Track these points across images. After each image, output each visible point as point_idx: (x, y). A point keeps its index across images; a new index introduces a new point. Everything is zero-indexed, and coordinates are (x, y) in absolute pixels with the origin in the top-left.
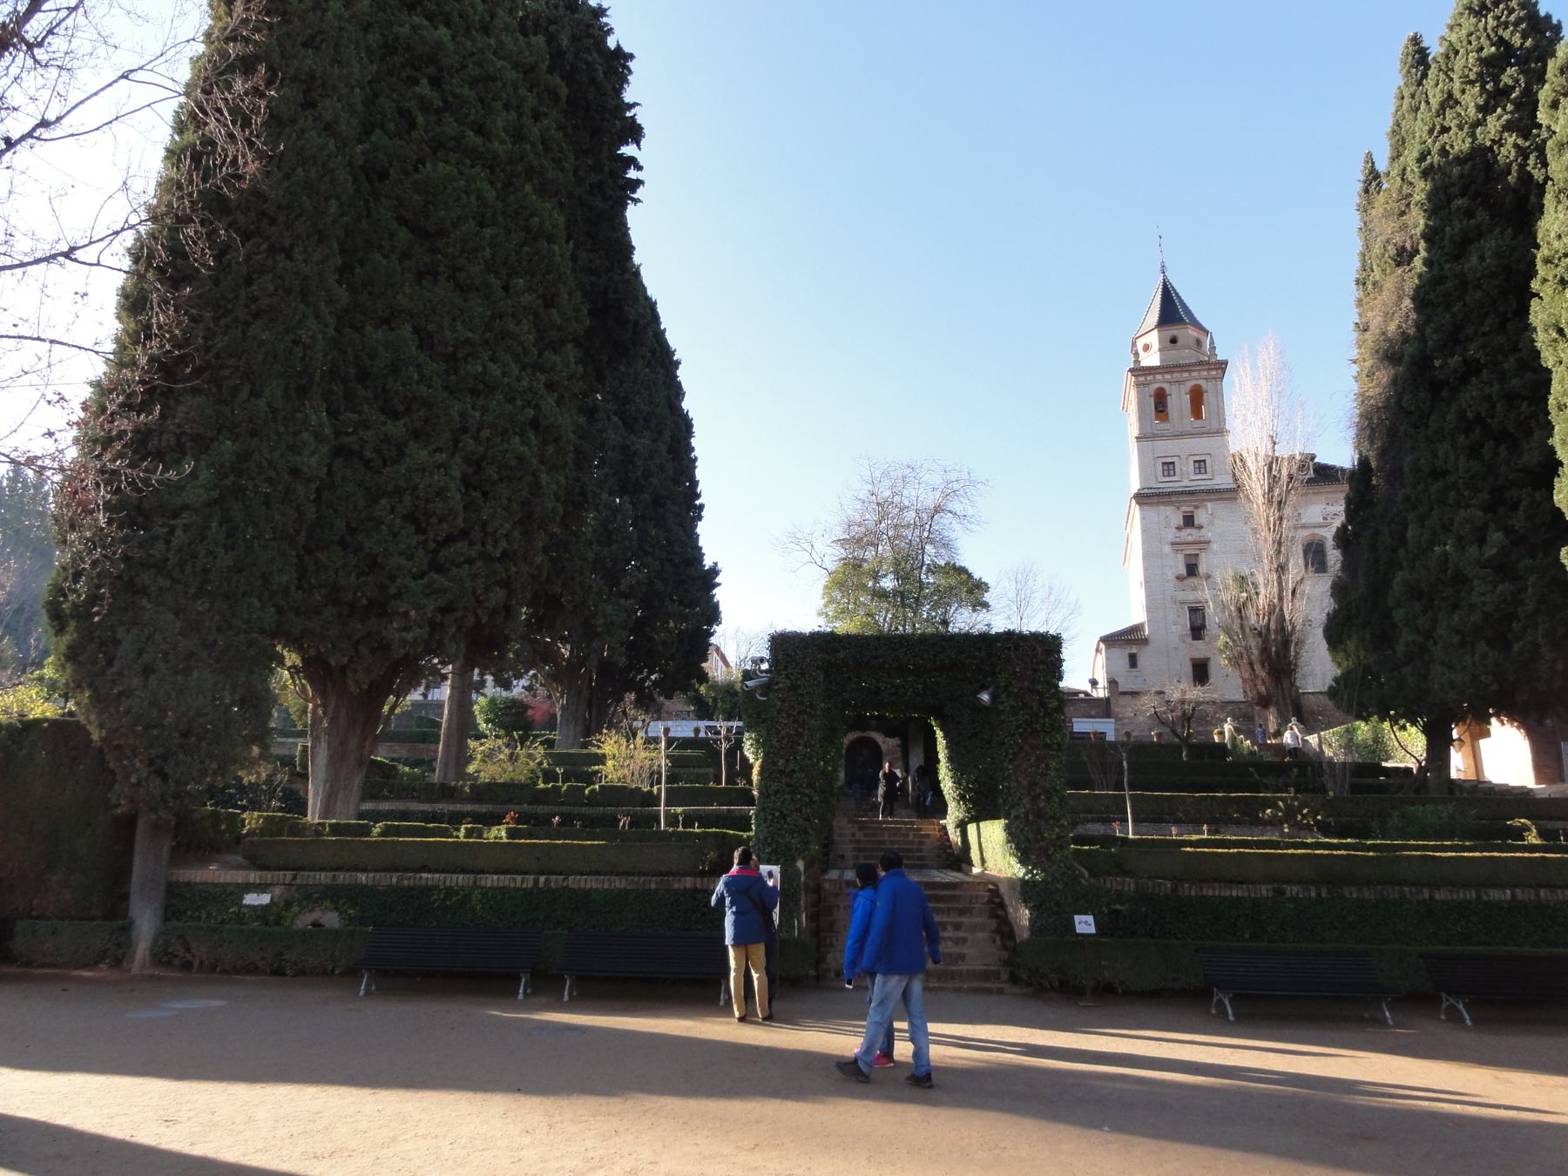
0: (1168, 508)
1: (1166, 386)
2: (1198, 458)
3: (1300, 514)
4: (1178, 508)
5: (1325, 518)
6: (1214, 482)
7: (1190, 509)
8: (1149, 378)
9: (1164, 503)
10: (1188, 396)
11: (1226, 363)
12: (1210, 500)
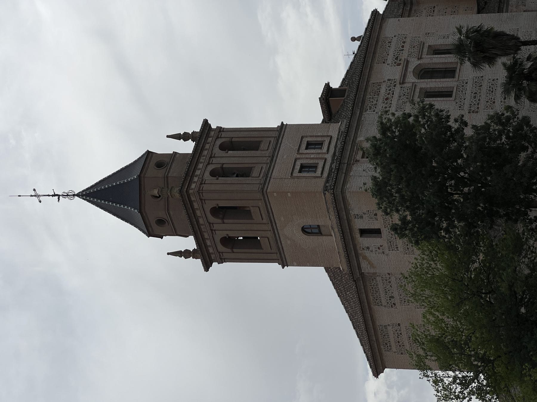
0: (354, 168)
1: (210, 168)
2: (304, 146)
3: (389, 80)
4: (357, 161)
5: (399, 65)
6: (335, 136)
7: (360, 153)
8: (196, 179)
9: (349, 169)
10: (229, 152)
11: (206, 122)
12: (355, 137)
